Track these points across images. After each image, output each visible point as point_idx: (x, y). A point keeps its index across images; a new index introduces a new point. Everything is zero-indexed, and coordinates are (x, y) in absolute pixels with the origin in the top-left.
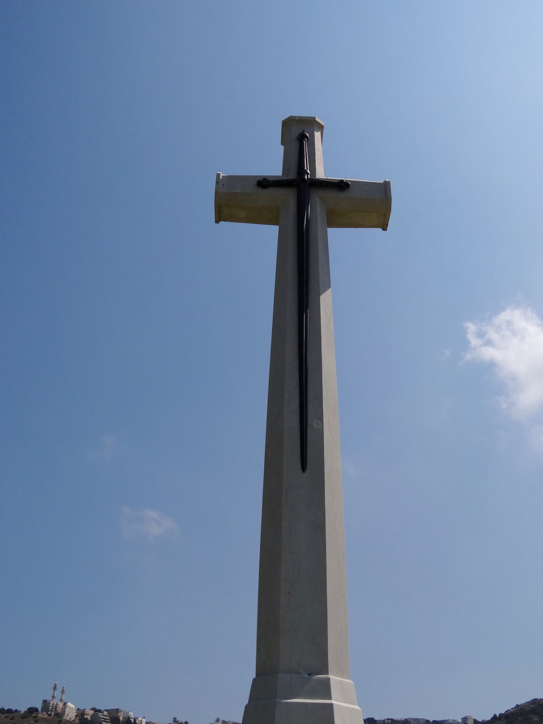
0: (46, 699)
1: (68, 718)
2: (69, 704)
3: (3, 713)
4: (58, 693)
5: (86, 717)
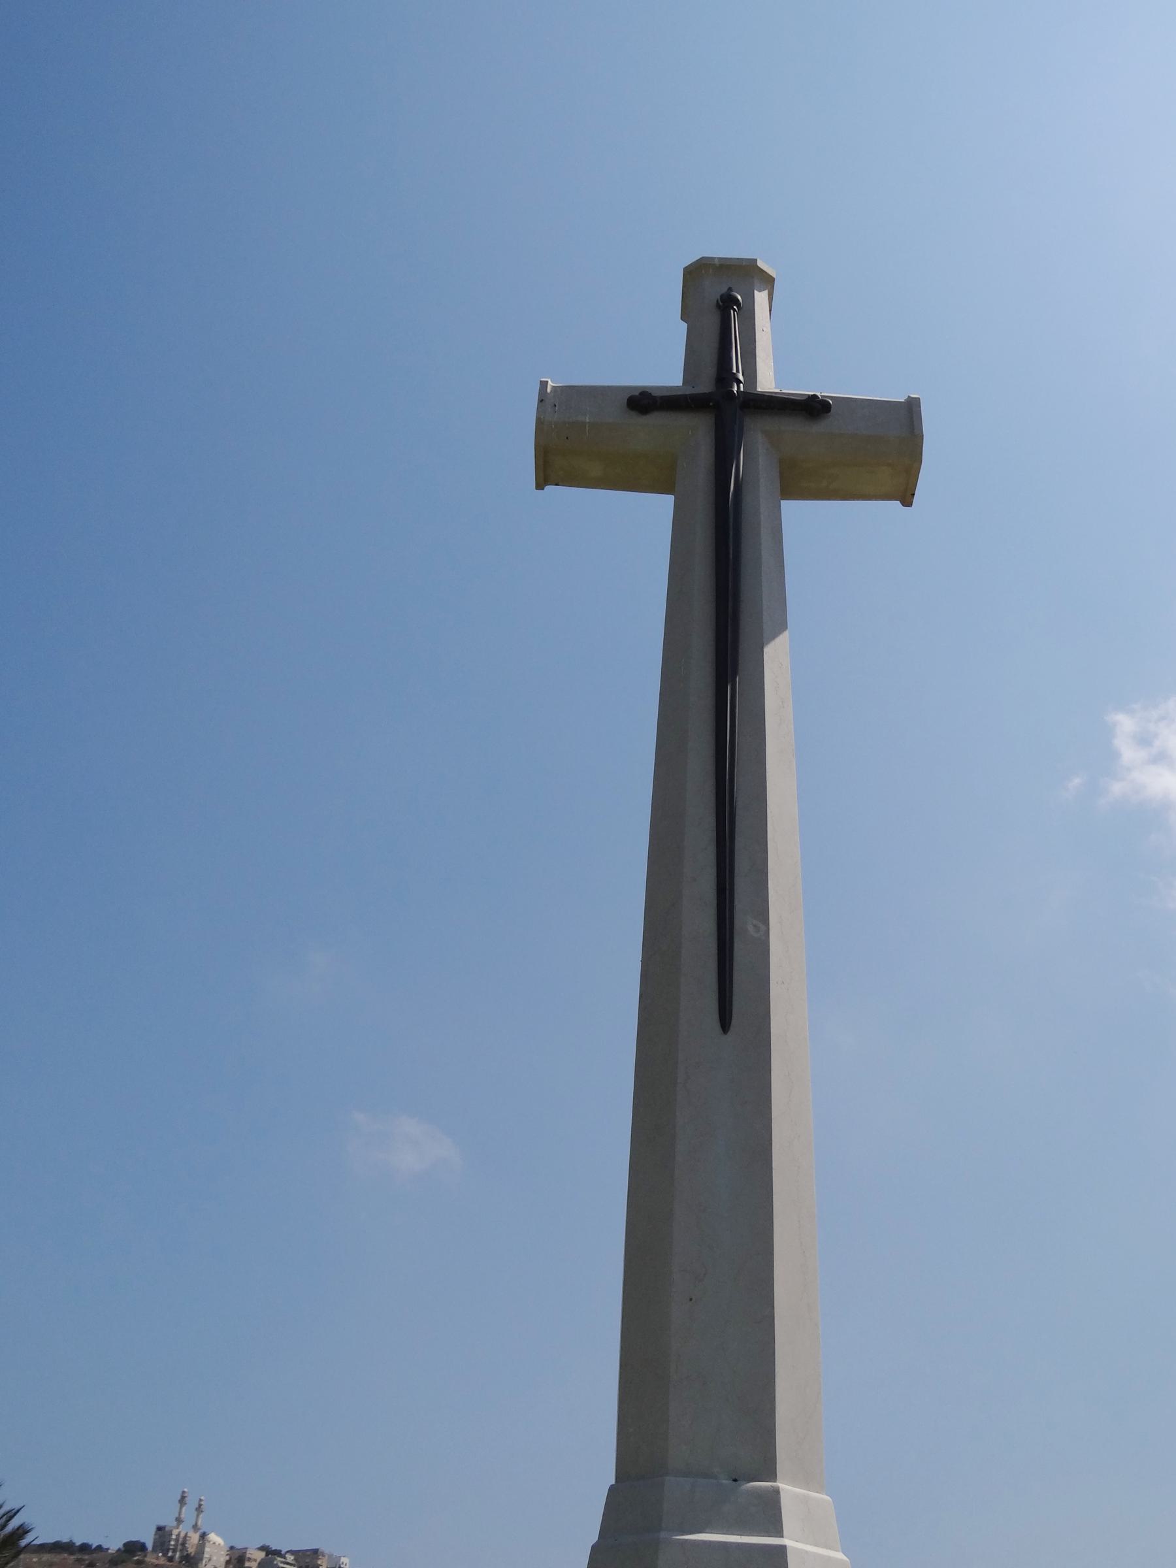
0: (162, 1524)
2: (213, 1537)
3: (72, 1553)
4: (188, 1513)
5: (247, 1564)
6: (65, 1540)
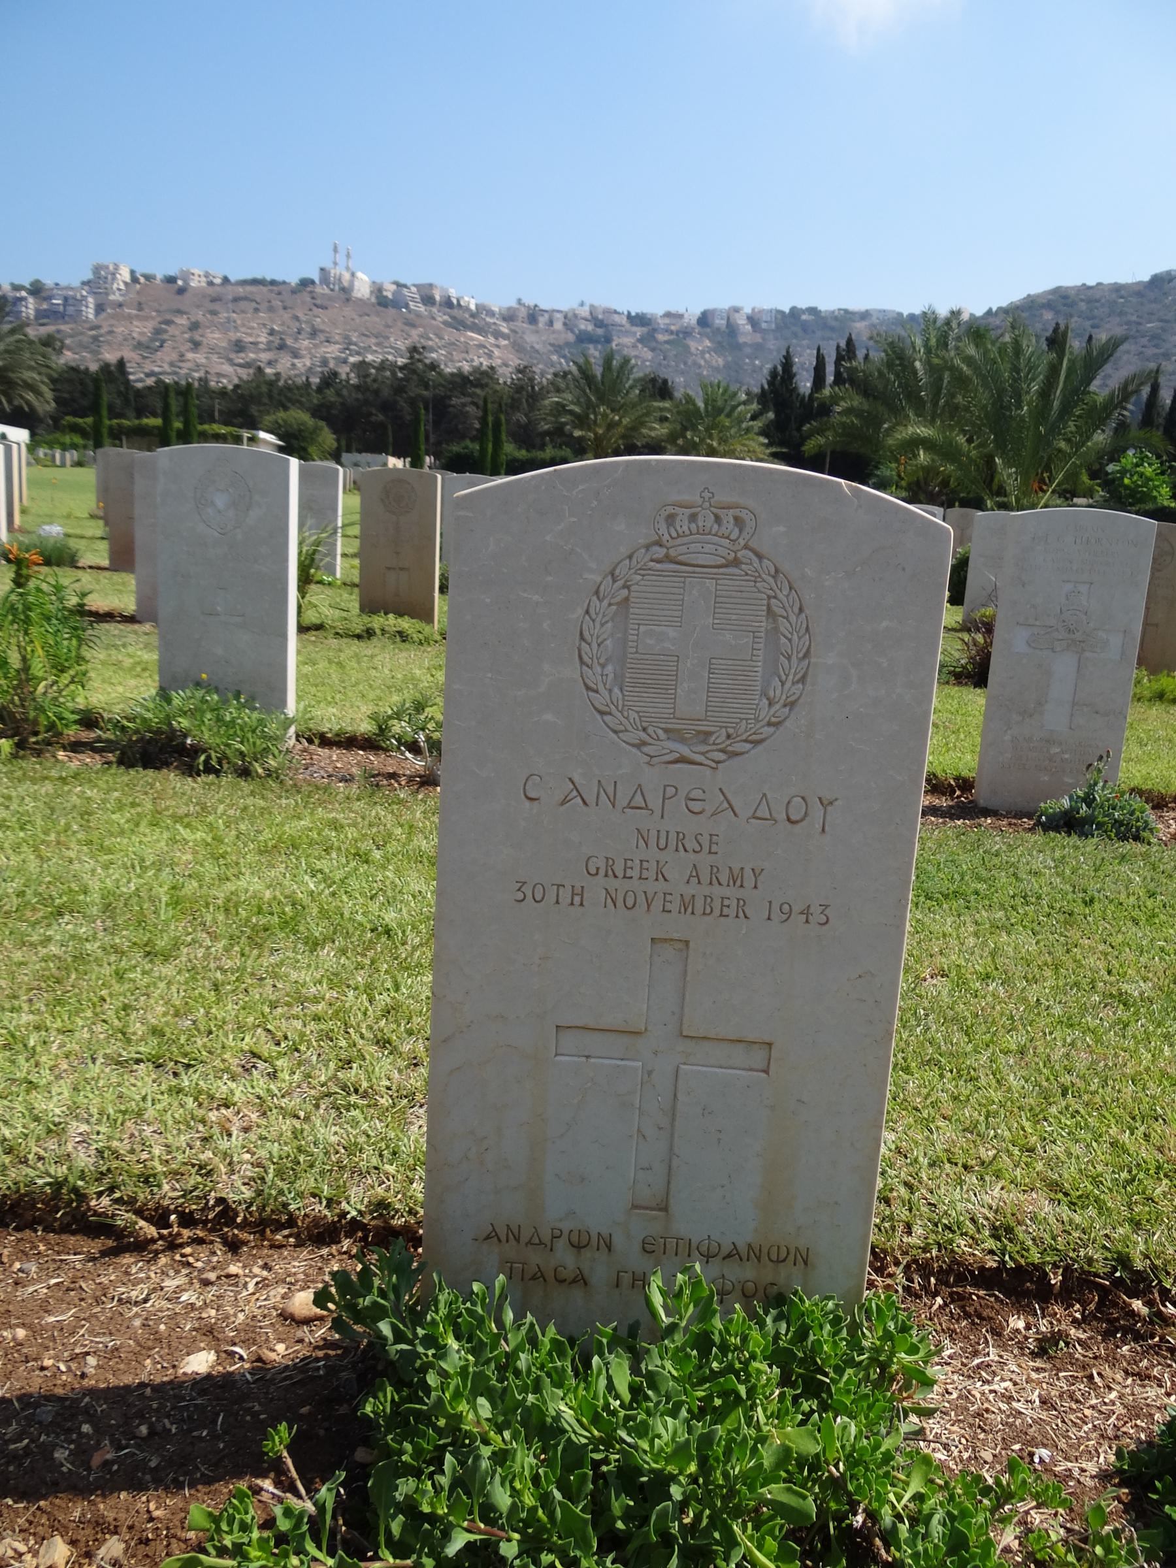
0: (323, 265)
1: (359, 295)
2: (360, 275)
4: (341, 258)
5: (385, 293)
6: (259, 276)
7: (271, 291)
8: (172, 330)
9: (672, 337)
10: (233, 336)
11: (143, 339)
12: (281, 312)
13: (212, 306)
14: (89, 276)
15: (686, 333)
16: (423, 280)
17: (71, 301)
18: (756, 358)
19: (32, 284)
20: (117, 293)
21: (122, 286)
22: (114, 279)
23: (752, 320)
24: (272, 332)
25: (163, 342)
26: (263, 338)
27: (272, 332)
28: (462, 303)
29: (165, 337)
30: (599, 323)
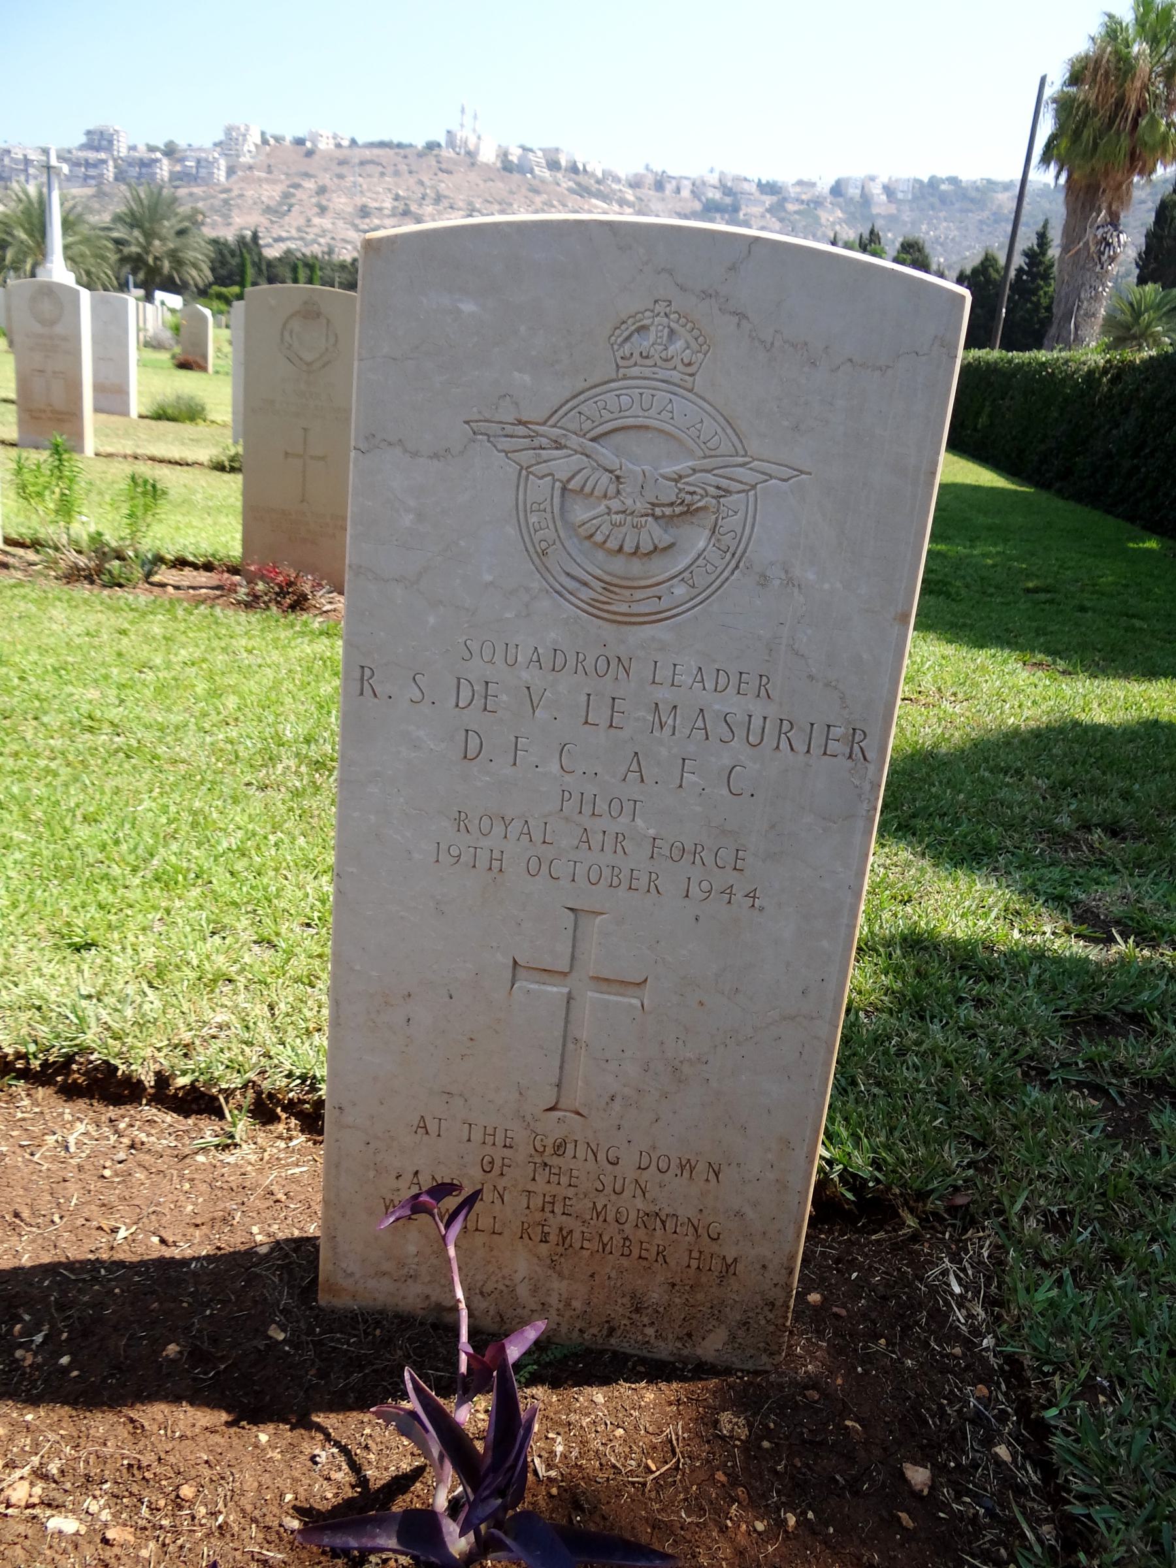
0: (449, 128)
4: (468, 119)
5: (510, 158)
6: (386, 139)
7: (397, 154)
8: (299, 194)
9: (802, 207)
10: (360, 201)
11: (272, 204)
12: (407, 175)
13: (338, 170)
14: (220, 136)
15: (818, 202)
16: (550, 144)
17: (203, 164)
18: (889, 230)
19: (166, 145)
20: (248, 155)
21: (253, 149)
22: (245, 140)
23: (888, 190)
24: (397, 198)
25: (291, 206)
26: (388, 204)
27: (397, 198)
28: (589, 168)
29: (293, 201)
30: (727, 191)
